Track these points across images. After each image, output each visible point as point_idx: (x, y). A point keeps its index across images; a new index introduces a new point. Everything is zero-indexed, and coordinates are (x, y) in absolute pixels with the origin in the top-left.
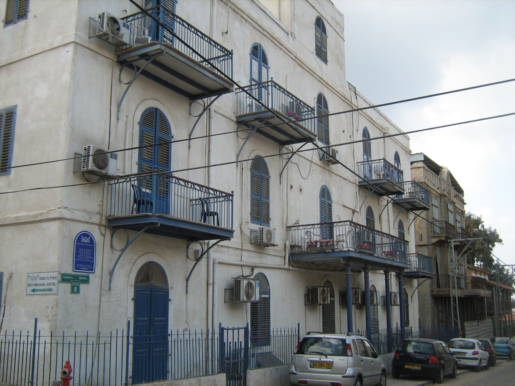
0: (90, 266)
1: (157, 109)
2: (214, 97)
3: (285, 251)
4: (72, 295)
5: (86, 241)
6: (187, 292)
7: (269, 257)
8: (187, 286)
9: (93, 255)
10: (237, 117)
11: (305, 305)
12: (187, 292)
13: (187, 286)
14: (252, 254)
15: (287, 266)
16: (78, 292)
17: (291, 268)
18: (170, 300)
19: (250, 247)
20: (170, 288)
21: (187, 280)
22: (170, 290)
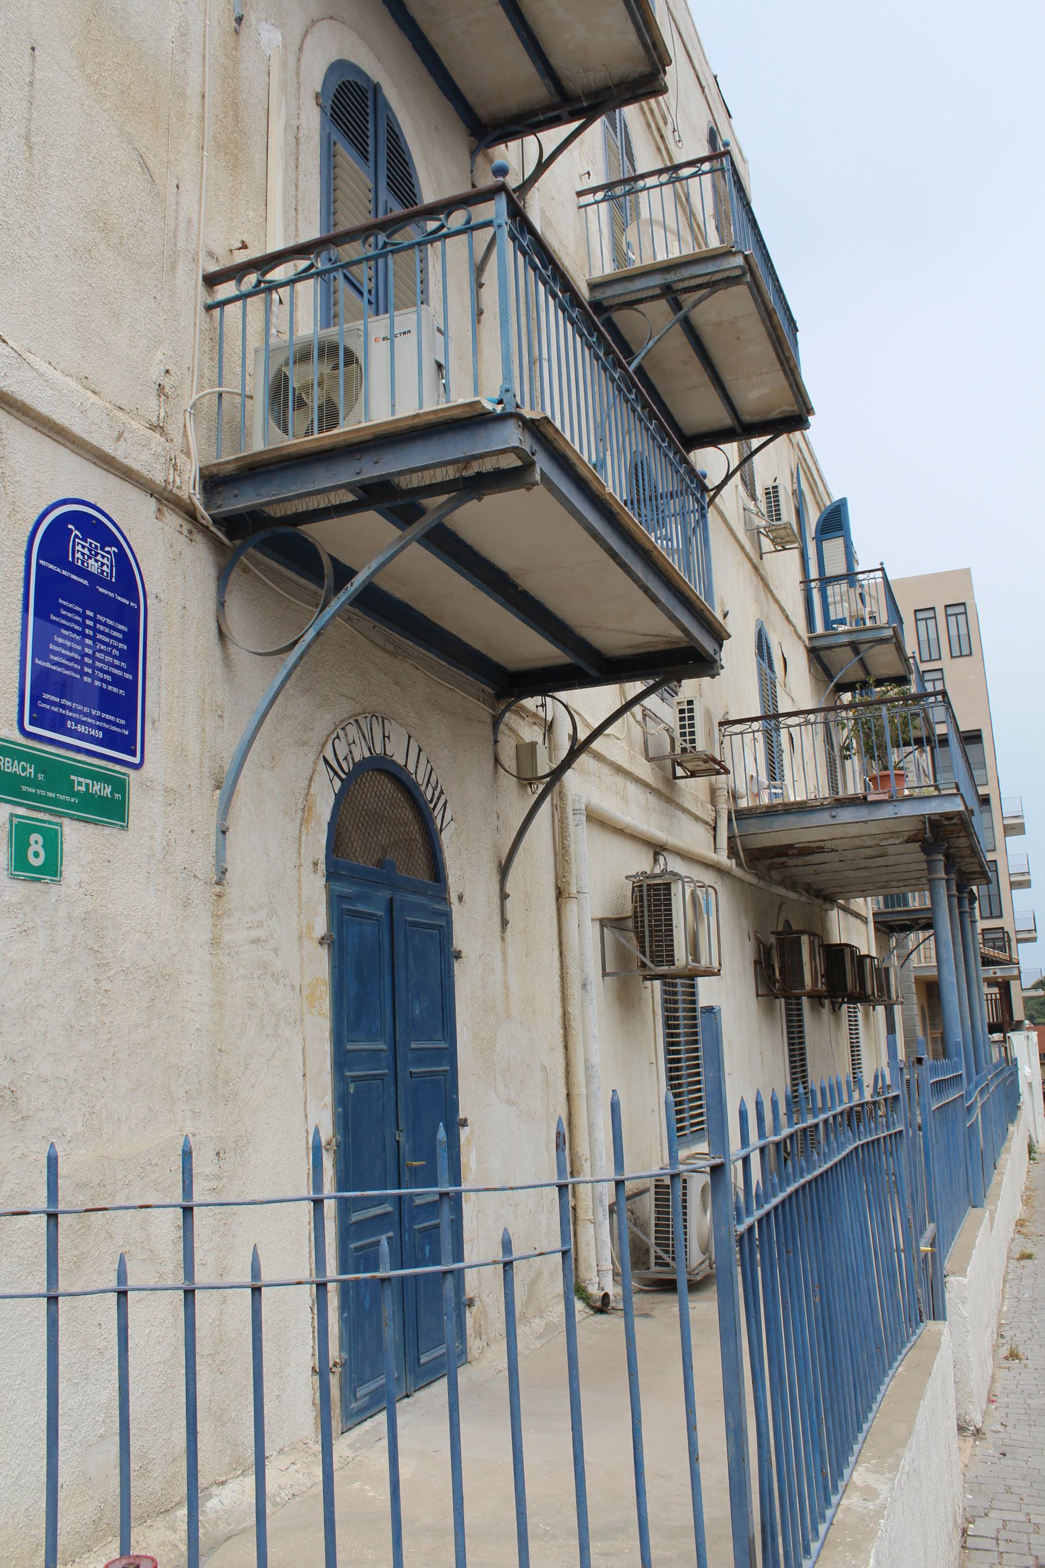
0: (117, 724)
1: (376, 88)
2: (575, 125)
3: (713, 802)
4: (22, 889)
5: (93, 566)
6: (504, 923)
7: (685, 821)
8: (504, 896)
9: (131, 650)
10: (593, 287)
11: (758, 995)
12: (504, 923)
13: (504, 896)
14: (653, 800)
15: (722, 857)
16: (52, 869)
17: (731, 864)
18: (458, 955)
19: (644, 770)
20: (453, 897)
21: (504, 870)
22: (455, 907)
